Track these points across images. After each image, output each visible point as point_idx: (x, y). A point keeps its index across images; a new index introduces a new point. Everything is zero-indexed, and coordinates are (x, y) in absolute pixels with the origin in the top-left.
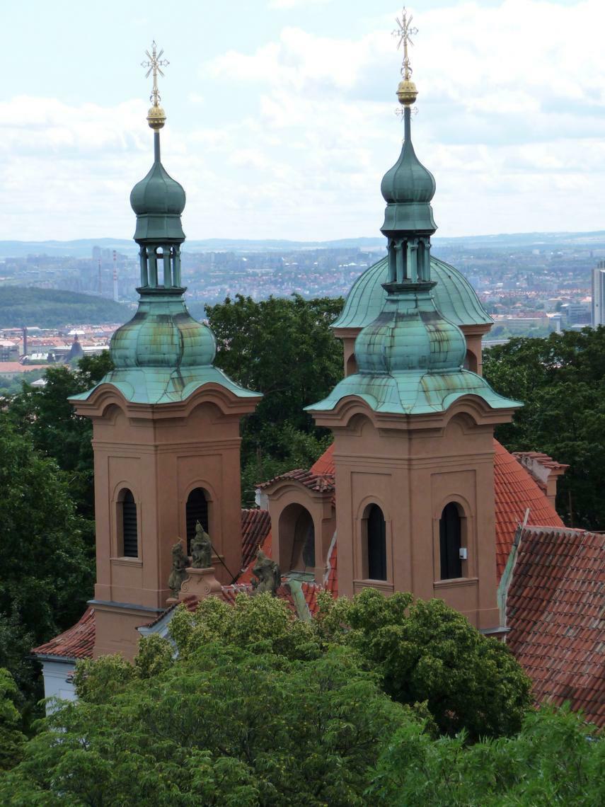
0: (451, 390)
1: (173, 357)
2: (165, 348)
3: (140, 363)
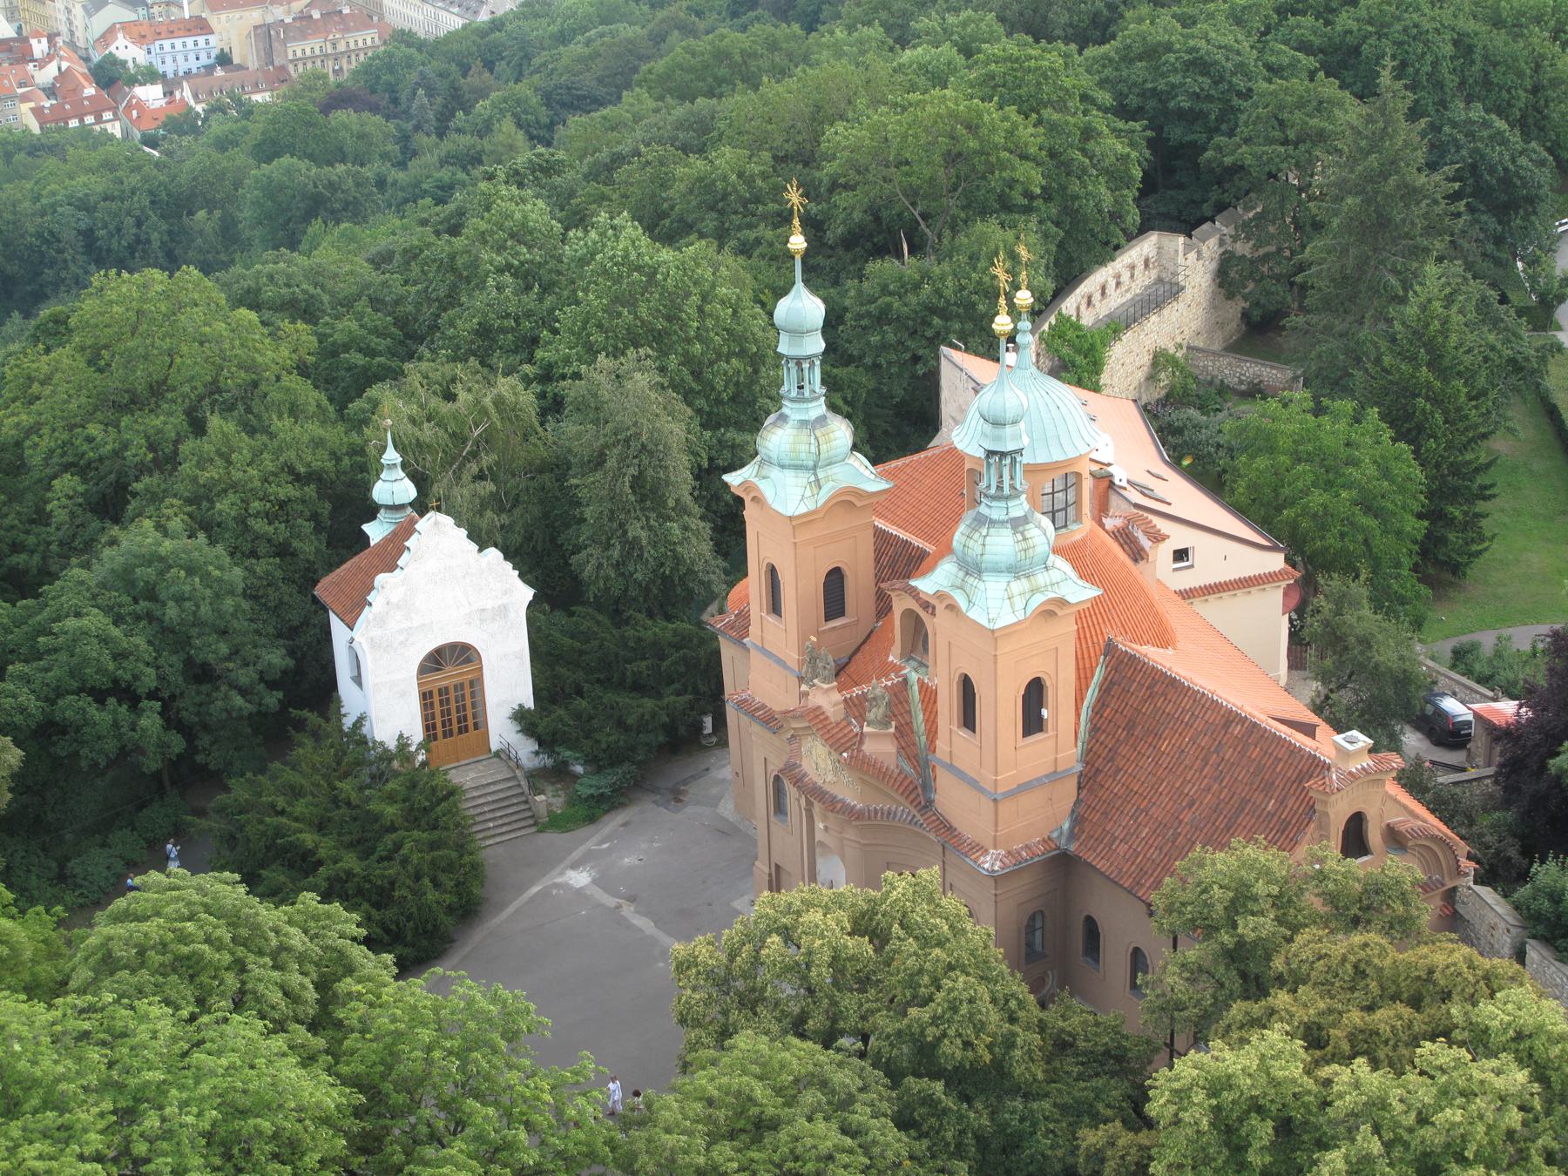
0: (1034, 591)
1: (811, 463)
2: (803, 456)
3: (783, 467)
